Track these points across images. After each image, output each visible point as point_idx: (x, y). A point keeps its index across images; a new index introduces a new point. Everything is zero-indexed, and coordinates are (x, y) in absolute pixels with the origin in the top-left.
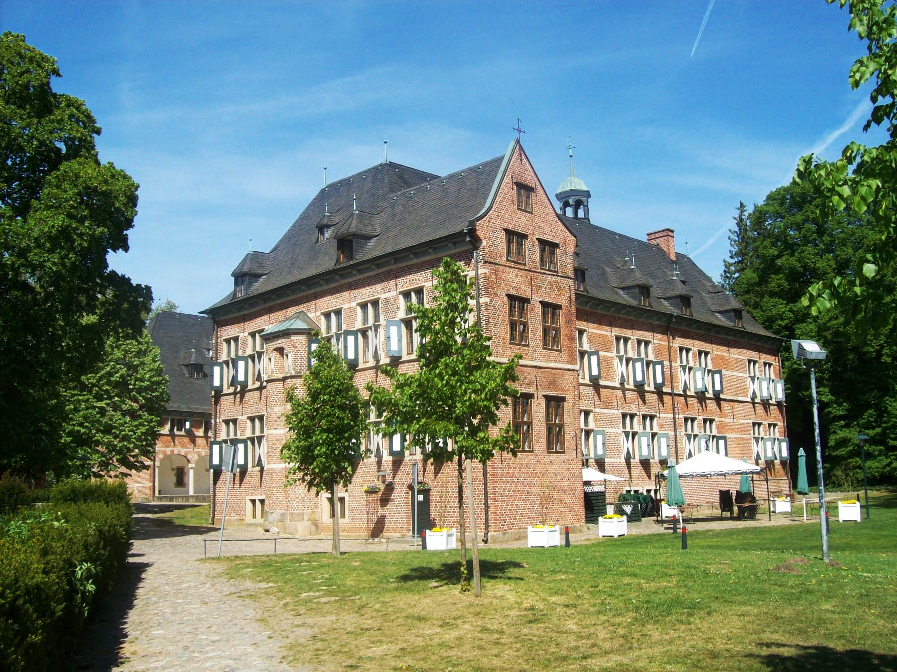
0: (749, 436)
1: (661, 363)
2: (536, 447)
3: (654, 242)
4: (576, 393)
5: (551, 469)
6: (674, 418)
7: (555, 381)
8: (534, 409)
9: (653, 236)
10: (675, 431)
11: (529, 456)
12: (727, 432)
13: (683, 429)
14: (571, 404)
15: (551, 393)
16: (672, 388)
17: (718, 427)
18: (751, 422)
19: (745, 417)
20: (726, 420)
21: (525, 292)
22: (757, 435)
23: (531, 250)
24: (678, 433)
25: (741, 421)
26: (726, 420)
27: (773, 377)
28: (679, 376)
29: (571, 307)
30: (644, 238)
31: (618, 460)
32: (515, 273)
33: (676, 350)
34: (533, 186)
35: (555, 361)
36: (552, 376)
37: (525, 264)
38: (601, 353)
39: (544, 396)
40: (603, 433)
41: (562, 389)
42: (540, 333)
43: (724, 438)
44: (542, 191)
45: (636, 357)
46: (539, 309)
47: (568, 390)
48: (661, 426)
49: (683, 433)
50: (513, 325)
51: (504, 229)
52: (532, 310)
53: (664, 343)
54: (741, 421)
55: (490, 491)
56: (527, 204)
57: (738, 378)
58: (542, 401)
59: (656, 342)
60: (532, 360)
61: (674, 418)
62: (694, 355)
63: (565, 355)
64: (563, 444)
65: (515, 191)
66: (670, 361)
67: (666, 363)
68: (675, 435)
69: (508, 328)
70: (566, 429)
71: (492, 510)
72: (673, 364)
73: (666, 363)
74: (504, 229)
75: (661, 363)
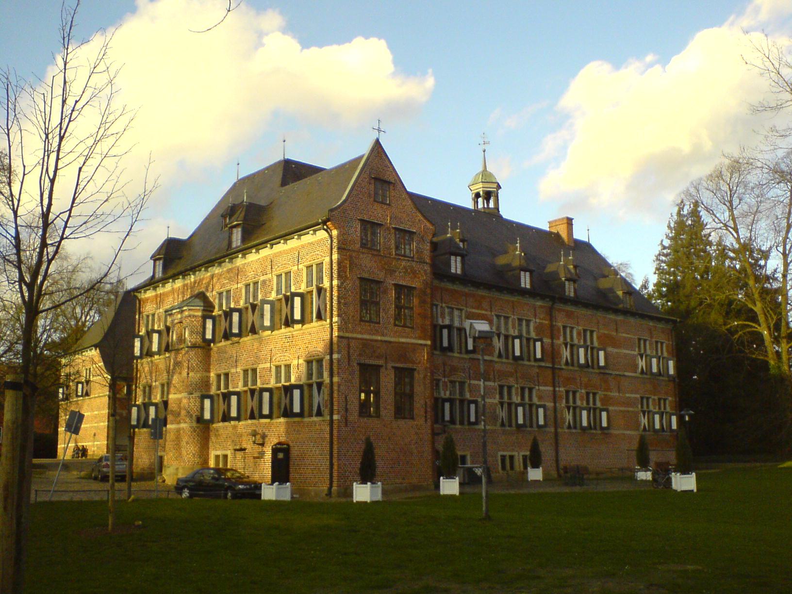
0: (636, 410)
1: (541, 340)
2: (383, 412)
3: (554, 230)
6: (554, 391)
8: (382, 379)
9: (554, 224)
10: (555, 403)
11: (375, 420)
12: (613, 405)
14: (422, 376)
15: (401, 365)
16: (553, 363)
17: (601, 400)
18: (638, 396)
19: (632, 392)
20: (612, 394)
21: (380, 275)
22: (645, 408)
23: (385, 240)
24: (557, 405)
25: (627, 395)
26: (612, 394)
27: (665, 354)
28: (562, 353)
30: (546, 227)
33: (559, 329)
35: (407, 337)
36: (403, 352)
37: (379, 251)
39: (393, 367)
40: (475, 402)
41: (413, 362)
42: (392, 311)
43: (607, 410)
45: (516, 334)
48: (540, 398)
49: (564, 404)
51: (359, 220)
53: (547, 322)
54: (627, 395)
55: (335, 451)
56: (384, 196)
57: (626, 355)
59: (538, 321)
60: (383, 335)
61: (554, 391)
62: (579, 334)
64: (411, 410)
65: (372, 187)
66: (552, 338)
67: (546, 340)
68: (555, 408)
70: (416, 398)
71: (335, 467)
72: (555, 341)
73: (547, 340)
74: (359, 220)
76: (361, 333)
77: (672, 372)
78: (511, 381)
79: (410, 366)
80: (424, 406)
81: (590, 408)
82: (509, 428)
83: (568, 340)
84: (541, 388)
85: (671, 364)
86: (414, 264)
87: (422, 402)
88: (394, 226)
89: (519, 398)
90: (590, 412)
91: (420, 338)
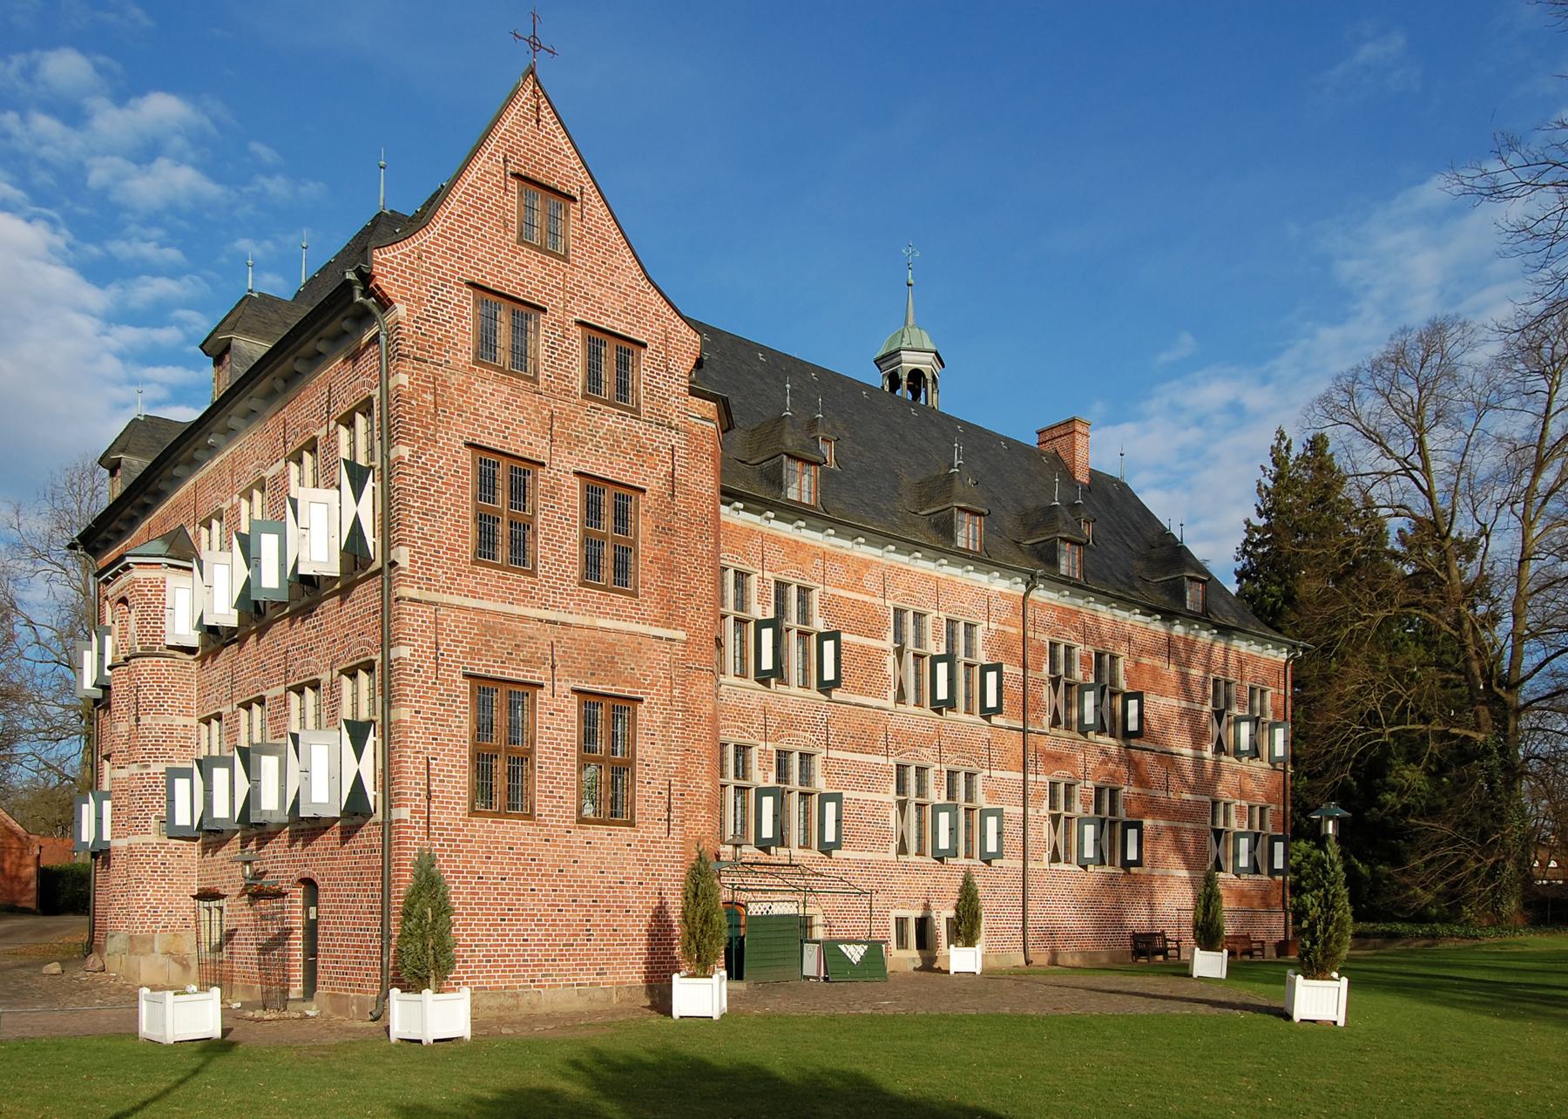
2: (542, 806)
3: (1047, 448)
4: (676, 692)
5: (590, 858)
7: (612, 662)
13: (1046, 803)
15: (600, 689)
29: (673, 496)
30: (1033, 441)
31: (881, 856)
32: (499, 398)
34: (575, 193)
35: (619, 617)
36: (605, 656)
38: (844, 637)
39: (575, 691)
44: (604, 211)
46: (574, 492)
47: (652, 685)
48: (992, 795)
50: (486, 524)
52: (552, 492)
58: (572, 707)
59: (993, 626)
63: (649, 606)
69: (471, 527)
75: (997, 668)
76: (474, 594)
77: (1279, 751)
78: (927, 756)
79: (626, 691)
80: (665, 794)
81: (1103, 821)
82: (918, 859)
83: (1062, 670)
84: (995, 774)
85: (1280, 735)
86: (639, 427)
87: (659, 784)
88: (578, 318)
89: (944, 793)
90: (1102, 827)
91: (655, 622)
